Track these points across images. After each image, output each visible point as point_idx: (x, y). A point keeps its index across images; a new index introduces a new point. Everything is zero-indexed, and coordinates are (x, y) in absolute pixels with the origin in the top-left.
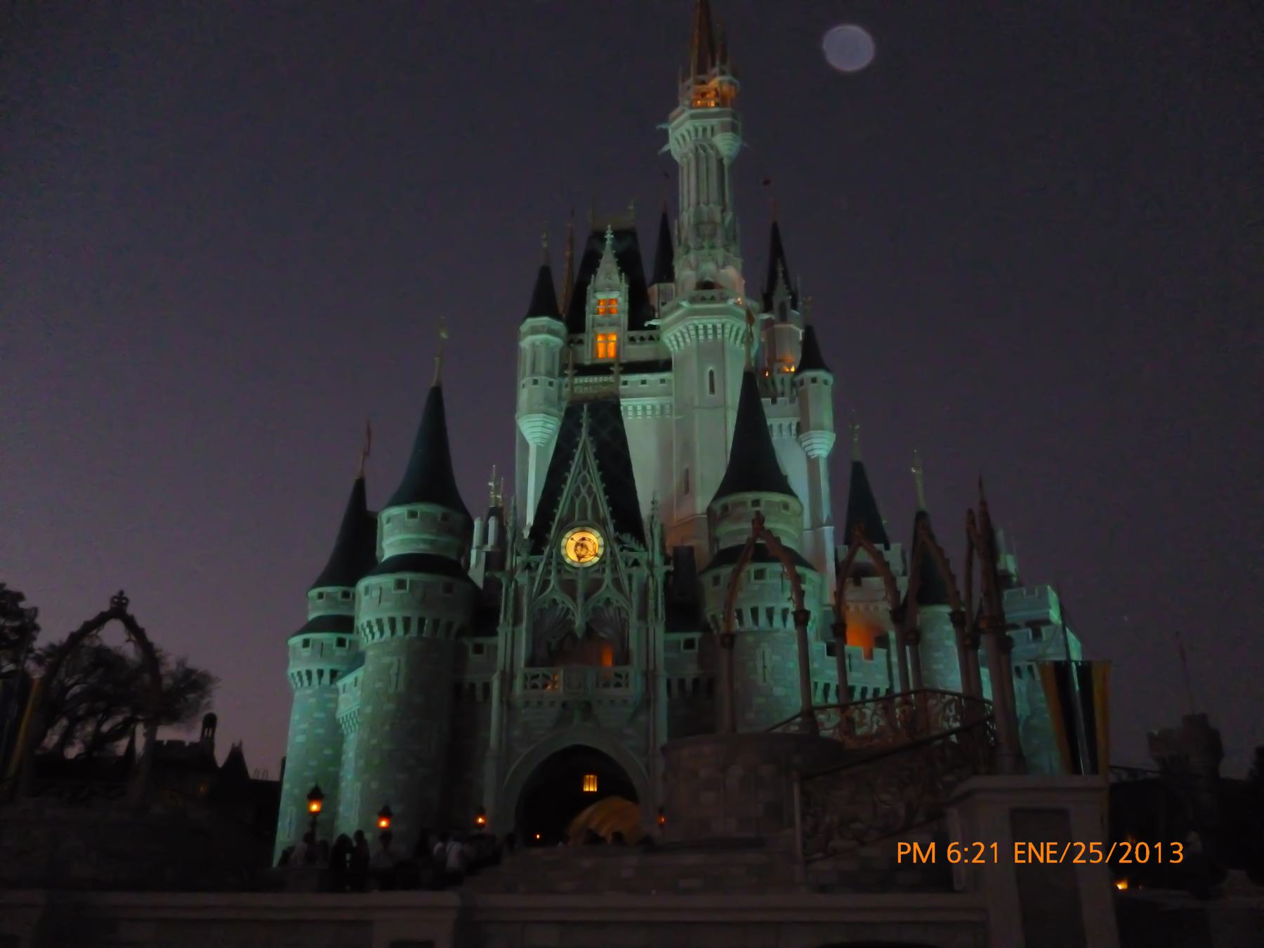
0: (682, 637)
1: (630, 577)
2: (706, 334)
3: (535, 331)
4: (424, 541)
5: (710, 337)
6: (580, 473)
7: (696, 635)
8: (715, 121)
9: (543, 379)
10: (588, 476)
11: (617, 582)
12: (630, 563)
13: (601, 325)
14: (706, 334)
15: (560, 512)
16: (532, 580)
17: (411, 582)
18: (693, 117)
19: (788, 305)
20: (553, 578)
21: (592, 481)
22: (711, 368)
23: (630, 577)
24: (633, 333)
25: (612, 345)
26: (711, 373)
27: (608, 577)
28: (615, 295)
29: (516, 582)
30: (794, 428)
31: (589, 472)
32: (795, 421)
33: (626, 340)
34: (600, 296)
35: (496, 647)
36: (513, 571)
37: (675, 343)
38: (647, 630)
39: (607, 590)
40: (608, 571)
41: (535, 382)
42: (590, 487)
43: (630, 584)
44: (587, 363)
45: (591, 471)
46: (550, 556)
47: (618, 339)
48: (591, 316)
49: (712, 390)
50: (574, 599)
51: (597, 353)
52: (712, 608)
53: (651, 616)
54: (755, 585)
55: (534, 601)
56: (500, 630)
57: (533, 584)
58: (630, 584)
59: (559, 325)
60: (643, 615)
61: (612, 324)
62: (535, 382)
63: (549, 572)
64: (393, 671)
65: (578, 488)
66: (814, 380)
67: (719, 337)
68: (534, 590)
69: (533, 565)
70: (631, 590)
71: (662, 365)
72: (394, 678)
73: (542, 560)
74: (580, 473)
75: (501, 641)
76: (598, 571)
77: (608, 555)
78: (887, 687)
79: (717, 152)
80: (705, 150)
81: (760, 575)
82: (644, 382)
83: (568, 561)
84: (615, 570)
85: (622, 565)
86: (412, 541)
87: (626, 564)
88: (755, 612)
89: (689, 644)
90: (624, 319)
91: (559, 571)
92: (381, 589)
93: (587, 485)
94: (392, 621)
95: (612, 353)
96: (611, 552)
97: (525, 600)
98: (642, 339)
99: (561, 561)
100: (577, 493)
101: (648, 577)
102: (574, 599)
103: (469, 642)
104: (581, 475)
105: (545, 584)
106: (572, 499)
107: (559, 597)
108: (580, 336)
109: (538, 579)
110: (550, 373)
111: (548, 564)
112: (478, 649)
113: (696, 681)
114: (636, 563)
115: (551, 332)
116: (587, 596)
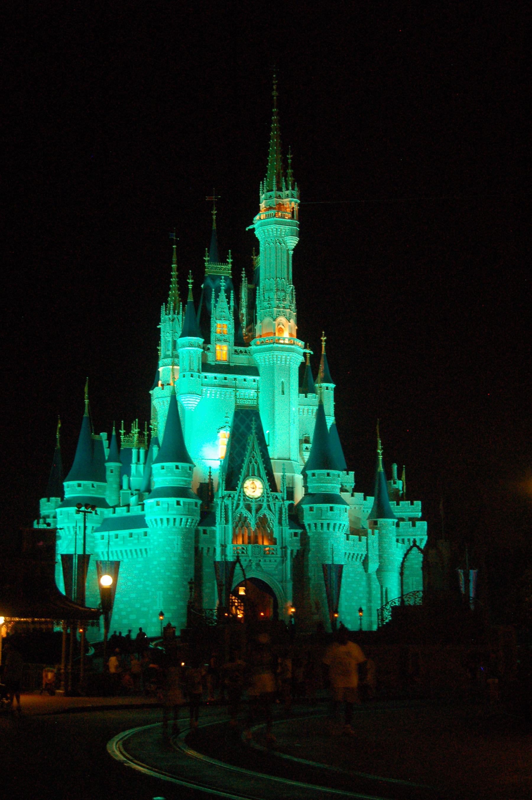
0: (293, 531)
1: (274, 504)
2: (281, 361)
3: (191, 345)
4: (183, 480)
5: (283, 362)
6: (251, 452)
7: (299, 531)
8: (287, 228)
9: (196, 374)
10: (255, 454)
11: (269, 506)
12: (275, 497)
13: (219, 340)
14: (281, 361)
15: (243, 471)
16: (233, 504)
17: (184, 502)
18: (276, 223)
20: (241, 503)
21: (257, 457)
22: (283, 380)
23: (274, 504)
25: (224, 352)
26: (282, 382)
27: (265, 505)
28: (227, 323)
29: (225, 503)
31: (255, 452)
33: (233, 352)
34: (218, 322)
35: (214, 532)
36: (223, 498)
37: (263, 361)
38: (282, 529)
39: (264, 511)
40: (265, 500)
41: (192, 376)
42: (256, 460)
43: (275, 508)
45: (257, 451)
46: (240, 492)
48: (214, 334)
49: (283, 393)
50: (251, 512)
51: (217, 357)
52: (307, 519)
53: (283, 522)
54: (330, 513)
55: (234, 512)
56: (217, 525)
57: (233, 504)
58: (275, 508)
59: (201, 340)
60: (280, 523)
61: (225, 341)
62: (192, 376)
63: (239, 500)
64: (175, 543)
65: (251, 459)
66: (327, 388)
68: (234, 508)
69: (232, 496)
70: (275, 511)
71: (253, 370)
72: (176, 546)
73: (236, 493)
74: (251, 452)
75: (218, 528)
76: (260, 500)
77: (265, 493)
79: (287, 246)
80: (280, 244)
81: (331, 509)
82: (245, 380)
83: (247, 494)
84: (268, 501)
85: (271, 499)
86: (177, 480)
87: (273, 497)
88: (328, 524)
89: (296, 534)
90: (232, 339)
91: (244, 499)
92: (168, 504)
93: (255, 458)
94: (175, 519)
96: (267, 492)
97: (230, 513)
98: (241, 352)
99: (245, 496)
100: (251, 462)
101: (282, 505)
102: (251, 512)
103: (201, 528)
104: (252, 453)
105: (238, 505)
106: (248, 464)
107: (245, 513)
108: (209, 346)
109: (235, 502)
110: (199, 372)
111: (239, 496)
112: (205, 532)
113: (298, 550)
114: (277, 498)
115: (199, 346)
116: (257, 511)
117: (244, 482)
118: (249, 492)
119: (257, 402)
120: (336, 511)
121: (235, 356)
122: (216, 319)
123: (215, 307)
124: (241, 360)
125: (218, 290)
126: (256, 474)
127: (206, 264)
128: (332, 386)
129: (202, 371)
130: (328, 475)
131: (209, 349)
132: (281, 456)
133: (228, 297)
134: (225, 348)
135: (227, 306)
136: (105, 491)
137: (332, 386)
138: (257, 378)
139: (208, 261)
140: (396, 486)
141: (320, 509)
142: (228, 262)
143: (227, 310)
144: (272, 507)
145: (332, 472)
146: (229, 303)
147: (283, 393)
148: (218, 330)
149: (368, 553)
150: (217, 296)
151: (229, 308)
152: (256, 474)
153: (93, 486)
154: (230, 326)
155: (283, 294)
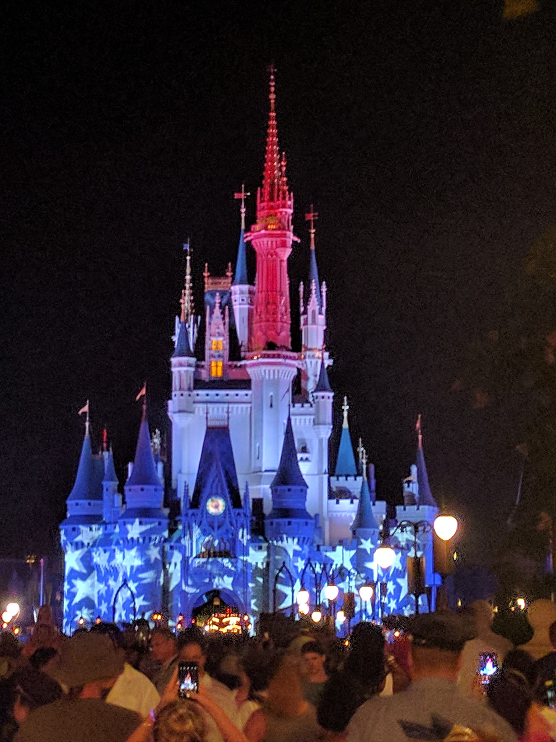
3: (181, 365)
9: (186, 393)
19: (317, 312)
22: (271, 394)
23: (236, 521)
24: (230, 363)
27: (228, 520)
28: (221, 339)
30: (312, 421)
32: (312, 417)
34: (214, 339)
44: (207, 380)
47: (223, 365)
49: (271, 406)
54: (288, 527)
62: (182, 395)
66: (323, 397)
67: (276, 377)
71: (245, 384)
78: (342, 563)
81: (289, 523)
84: (230, 517)
85: (233, 515)
91: (206, 517)
95: (220, 374)
99: (207, 513)
108: (203, 363)
110: (189, 389)
111: (202, 513)
115: (190, 365)
117: (206, 501)
118: (211, 509)
119: (228, 422)
120: (293, 525)
121: (229, 371)
122: (211, 335)
123: (210, 324)
124: (234, 374)
125: (212, 308)
126: (219, 492)
127: (206, 280)
128: (331, 394)
129: (195, 388)
130: (289, 490)
131: (203, 367)
132: (267, 469)
133: (223, 313)
134: (220, 364)
135: (221, 322)
136: (102, 508)
137: (331, 394)
138: (249, 392)
139: (208, 277)
140: (410, 490)
141: (278, 524)
142: (227, 276)
143: (222, 327)
144: (234, 522)
145: (293, 488)
146: (224, 318)
147: (271, 406)
148: (214, 347)
149: (343, 563)
150: (212, 313)
151: (224, 324)
152: (219, 492)
153: (90, 504)
154: (224, 342)
155: (274, 307)
